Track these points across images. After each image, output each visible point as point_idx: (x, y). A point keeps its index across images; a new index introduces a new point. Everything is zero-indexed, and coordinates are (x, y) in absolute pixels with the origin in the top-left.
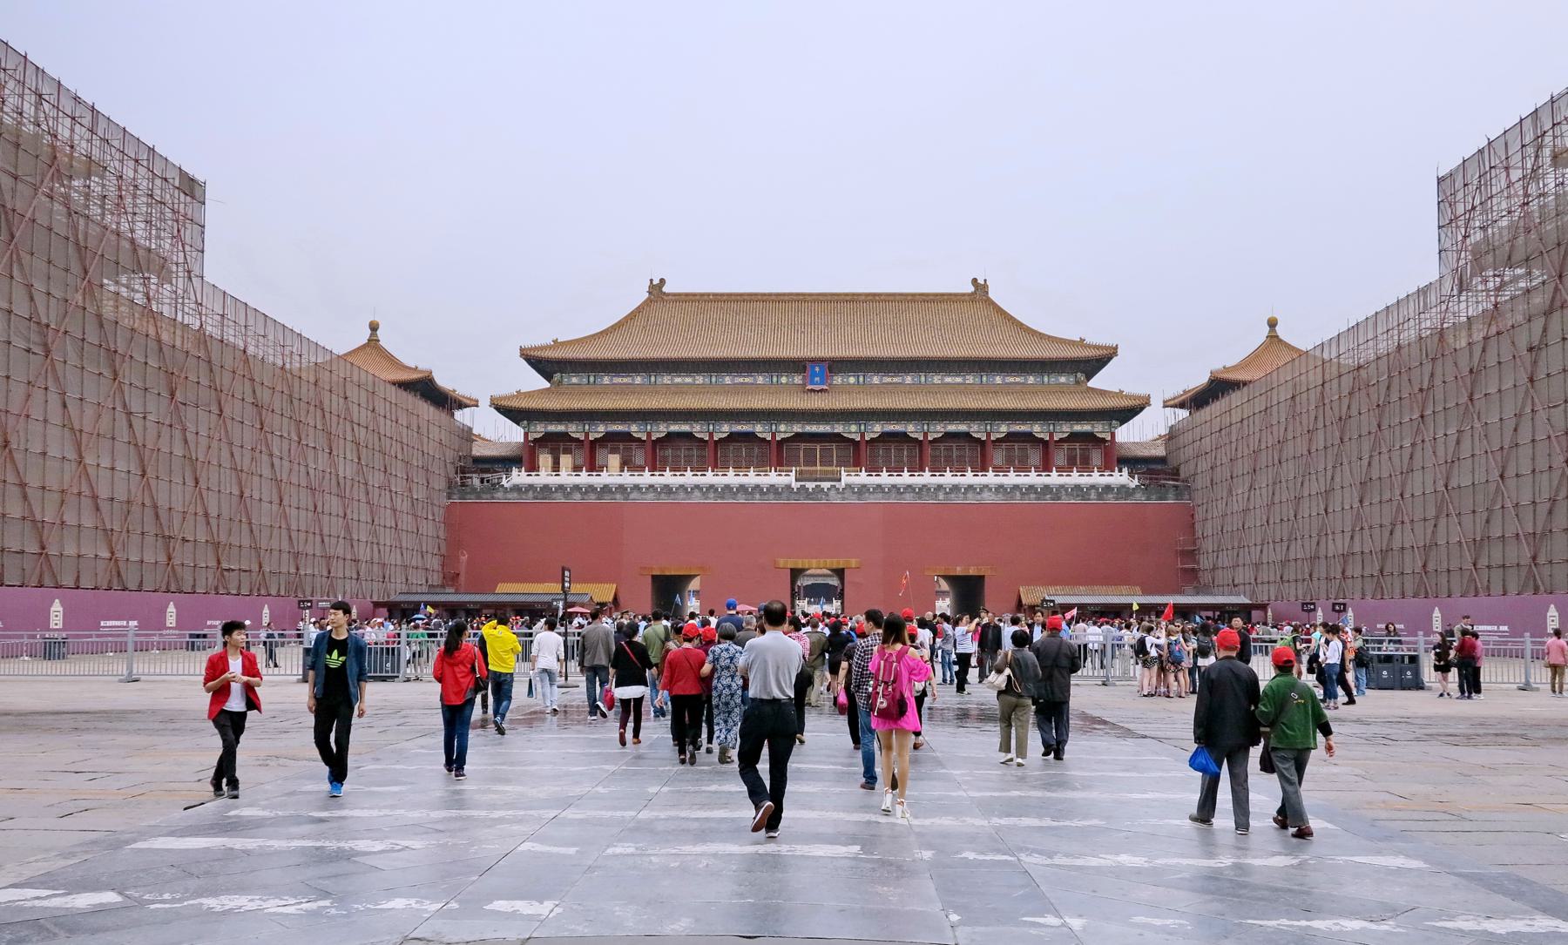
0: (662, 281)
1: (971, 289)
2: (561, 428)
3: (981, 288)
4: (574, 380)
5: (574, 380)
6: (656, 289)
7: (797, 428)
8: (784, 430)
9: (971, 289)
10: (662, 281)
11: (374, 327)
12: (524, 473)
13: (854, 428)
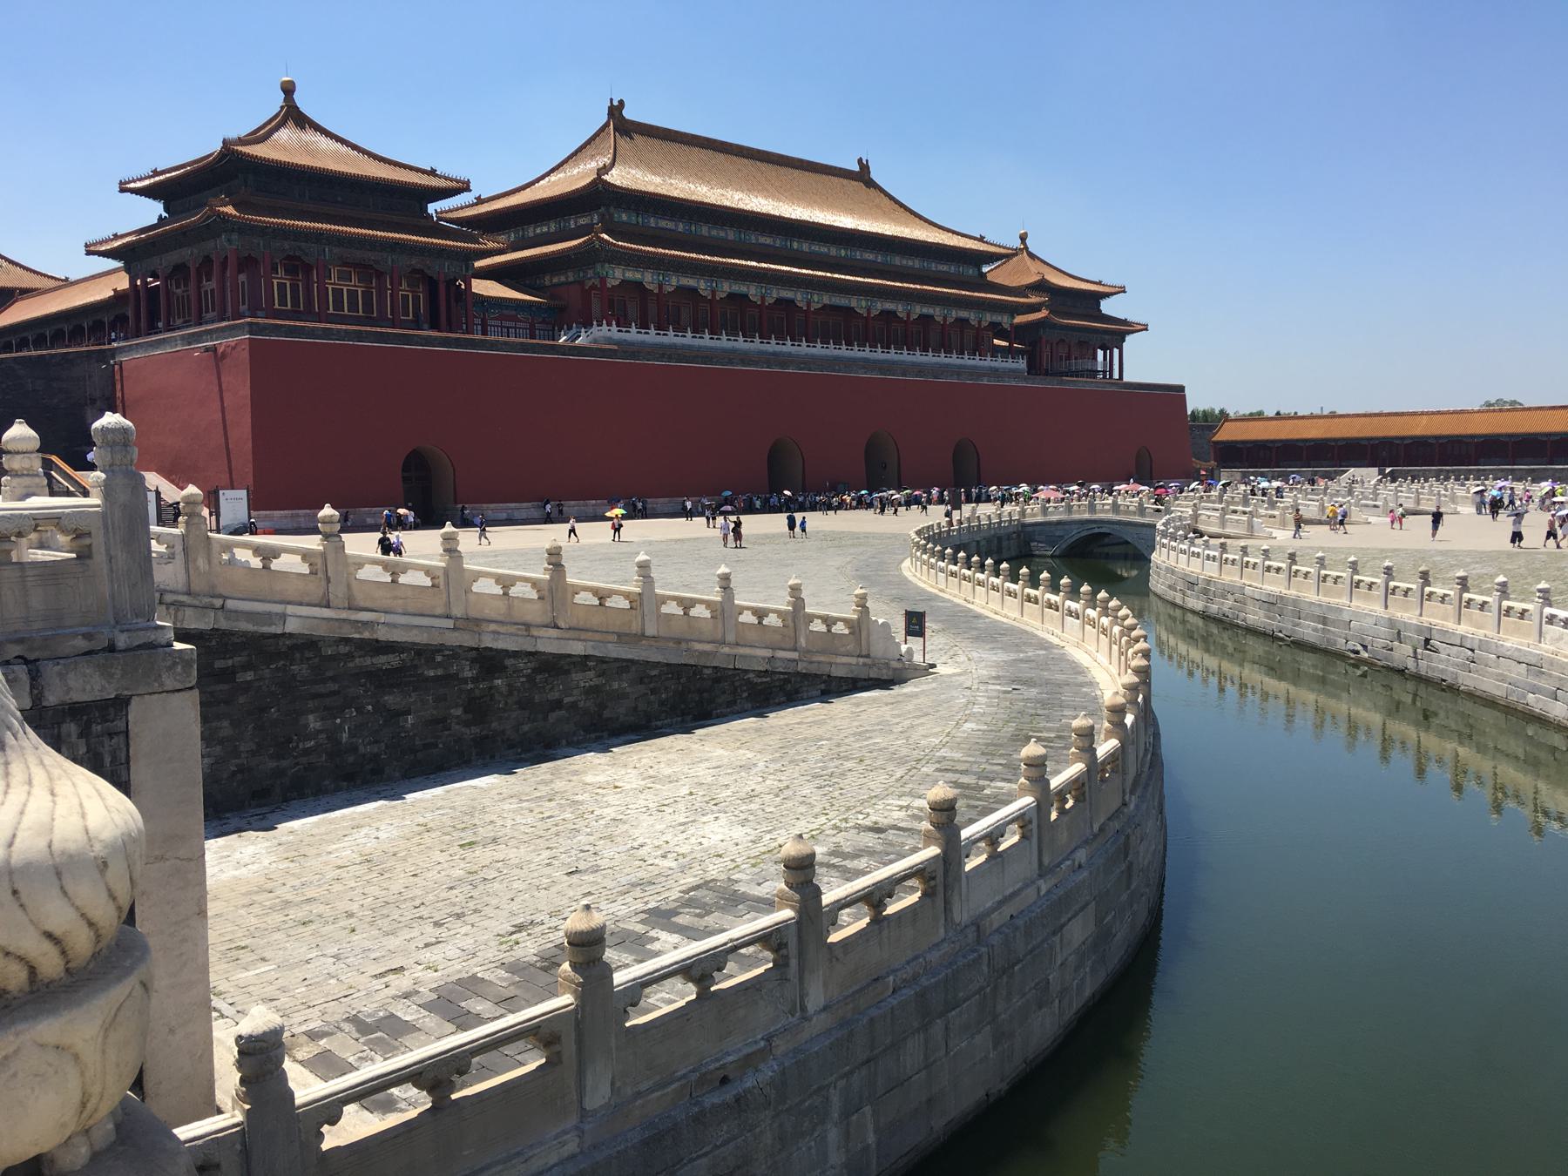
0: (621, 103)
1: (857, 168)
2: (638, 276)
3: (864, 167)
4: (624, 217)
5: (624, 217)
6: (615, 111)
7: (826, 300)
8: (820, 299)
9: (857, 168)
10: (621, 103)
11: (288, 89)
12: (614, 328)
13: (864, 303)
